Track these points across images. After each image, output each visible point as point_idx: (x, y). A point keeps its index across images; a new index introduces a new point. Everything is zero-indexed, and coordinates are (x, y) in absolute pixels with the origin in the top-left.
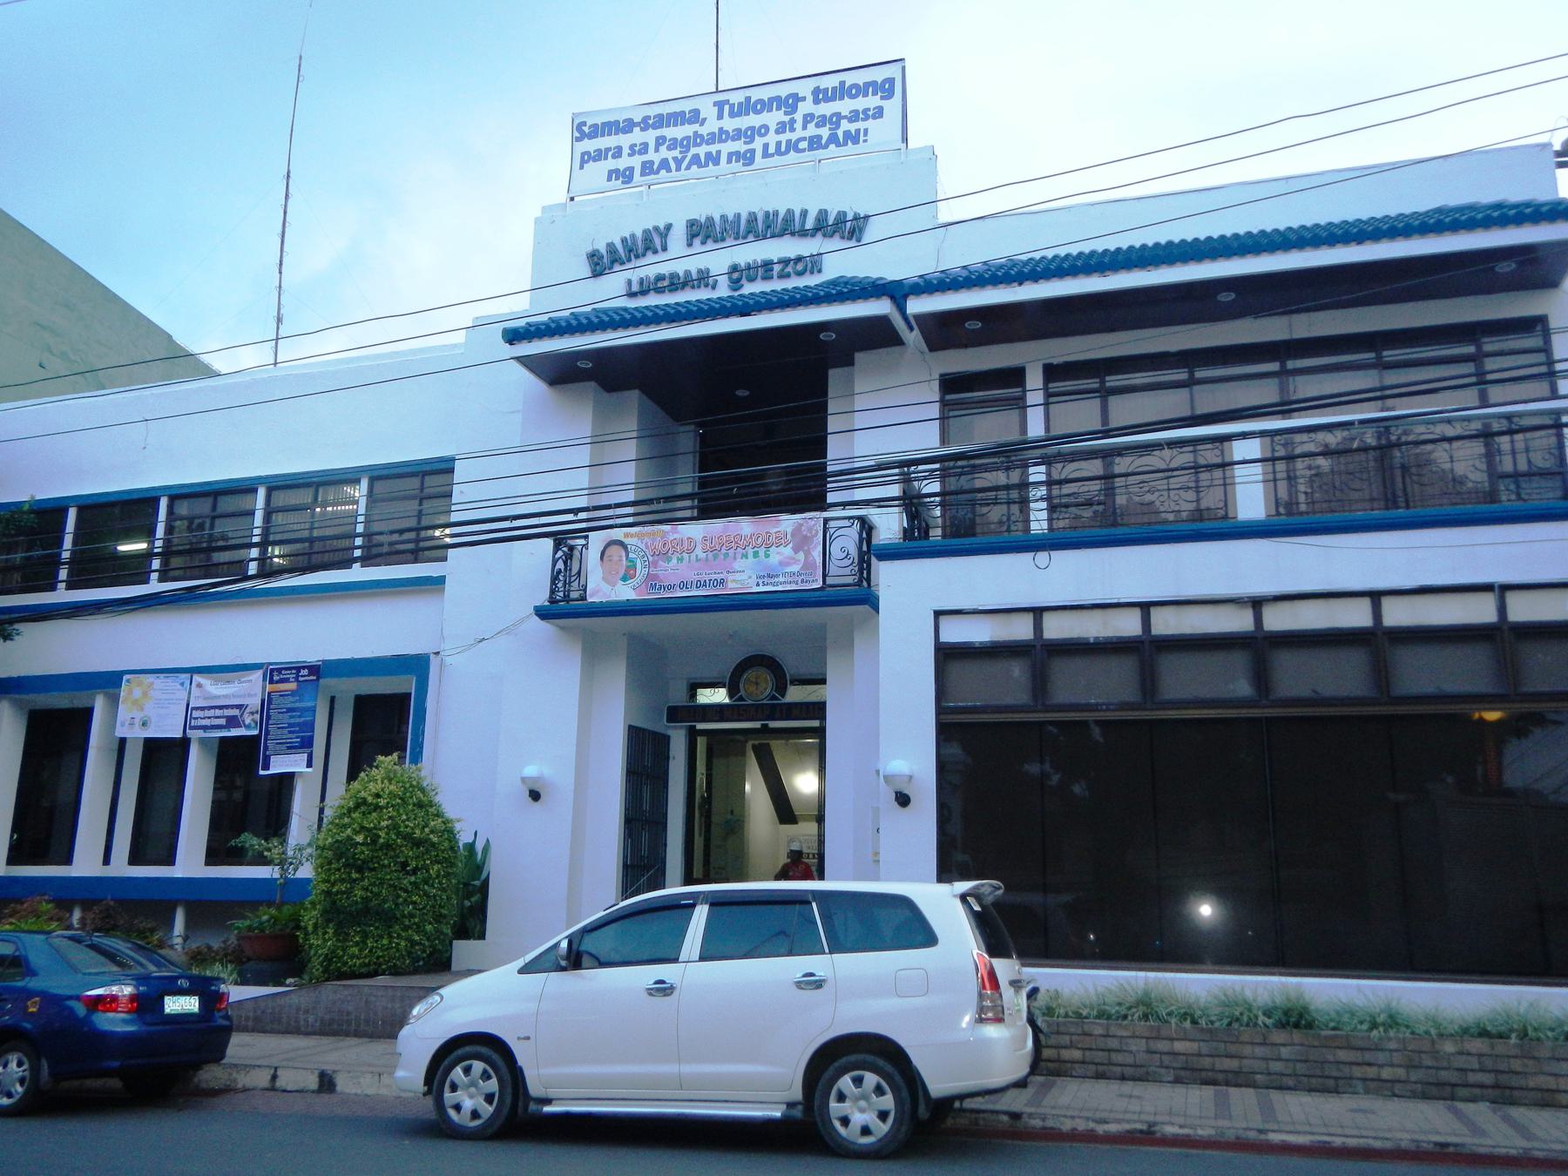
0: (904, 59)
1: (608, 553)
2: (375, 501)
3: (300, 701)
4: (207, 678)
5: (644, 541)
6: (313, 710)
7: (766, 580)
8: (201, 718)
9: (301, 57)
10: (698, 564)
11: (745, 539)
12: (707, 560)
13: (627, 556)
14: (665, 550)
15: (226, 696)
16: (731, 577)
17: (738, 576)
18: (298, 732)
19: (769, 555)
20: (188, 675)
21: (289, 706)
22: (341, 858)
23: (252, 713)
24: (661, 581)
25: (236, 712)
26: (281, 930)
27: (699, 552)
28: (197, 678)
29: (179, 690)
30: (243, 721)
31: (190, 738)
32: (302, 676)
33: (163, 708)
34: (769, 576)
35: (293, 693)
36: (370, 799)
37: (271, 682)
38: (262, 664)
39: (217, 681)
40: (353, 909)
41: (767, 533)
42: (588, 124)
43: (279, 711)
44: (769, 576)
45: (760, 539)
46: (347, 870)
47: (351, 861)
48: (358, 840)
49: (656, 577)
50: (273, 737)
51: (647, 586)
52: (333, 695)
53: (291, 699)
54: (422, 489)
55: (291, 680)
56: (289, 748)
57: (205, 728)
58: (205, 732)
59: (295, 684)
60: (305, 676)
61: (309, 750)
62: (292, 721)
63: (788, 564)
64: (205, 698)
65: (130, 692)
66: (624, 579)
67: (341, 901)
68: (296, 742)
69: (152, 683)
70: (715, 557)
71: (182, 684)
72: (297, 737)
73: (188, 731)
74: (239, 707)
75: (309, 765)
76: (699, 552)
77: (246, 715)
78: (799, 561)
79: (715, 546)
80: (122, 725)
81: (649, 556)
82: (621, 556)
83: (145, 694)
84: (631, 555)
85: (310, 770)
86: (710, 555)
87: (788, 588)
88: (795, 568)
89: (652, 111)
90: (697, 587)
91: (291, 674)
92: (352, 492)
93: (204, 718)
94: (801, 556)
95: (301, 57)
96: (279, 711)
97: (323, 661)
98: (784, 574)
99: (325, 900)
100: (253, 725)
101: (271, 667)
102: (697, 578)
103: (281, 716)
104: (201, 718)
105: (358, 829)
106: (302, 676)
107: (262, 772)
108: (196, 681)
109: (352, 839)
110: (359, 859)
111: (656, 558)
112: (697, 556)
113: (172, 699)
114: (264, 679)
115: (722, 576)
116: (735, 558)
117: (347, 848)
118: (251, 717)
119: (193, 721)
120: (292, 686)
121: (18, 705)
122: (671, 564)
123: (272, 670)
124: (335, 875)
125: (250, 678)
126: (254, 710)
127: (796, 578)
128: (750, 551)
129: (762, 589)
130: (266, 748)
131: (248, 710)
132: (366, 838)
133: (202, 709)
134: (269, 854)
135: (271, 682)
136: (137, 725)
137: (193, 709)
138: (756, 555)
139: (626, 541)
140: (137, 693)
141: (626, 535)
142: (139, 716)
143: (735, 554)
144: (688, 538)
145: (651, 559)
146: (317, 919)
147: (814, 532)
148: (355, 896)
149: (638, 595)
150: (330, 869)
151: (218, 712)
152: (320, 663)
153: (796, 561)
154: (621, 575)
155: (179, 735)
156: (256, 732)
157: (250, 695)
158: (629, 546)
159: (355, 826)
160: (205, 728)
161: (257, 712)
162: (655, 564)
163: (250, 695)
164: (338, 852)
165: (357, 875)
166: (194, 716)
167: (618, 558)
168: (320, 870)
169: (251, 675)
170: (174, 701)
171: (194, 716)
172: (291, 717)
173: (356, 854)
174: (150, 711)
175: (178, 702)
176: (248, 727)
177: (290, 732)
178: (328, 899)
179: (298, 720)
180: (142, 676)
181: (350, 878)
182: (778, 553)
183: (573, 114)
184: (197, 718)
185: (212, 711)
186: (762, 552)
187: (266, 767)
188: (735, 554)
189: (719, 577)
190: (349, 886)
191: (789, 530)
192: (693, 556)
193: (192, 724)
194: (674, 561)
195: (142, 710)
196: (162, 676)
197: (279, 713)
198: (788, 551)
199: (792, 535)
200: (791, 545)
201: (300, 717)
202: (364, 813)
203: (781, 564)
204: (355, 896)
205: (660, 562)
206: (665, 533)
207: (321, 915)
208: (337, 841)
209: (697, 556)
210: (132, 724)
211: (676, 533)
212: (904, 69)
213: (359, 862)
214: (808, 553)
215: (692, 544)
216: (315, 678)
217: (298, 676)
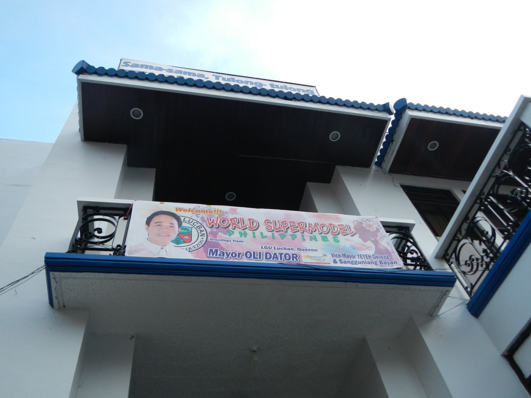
0: (315, 87)
1: (156, 219)
5: (200, 216)
7: (342, 258)
10: (264, 240)
11: (310, 226)
12: (273, 237)
13: (180, 225)
14: (226, 224)
16: (303, 254)
17: (311, 254)
19: (338, 241)
24: (222, 248)
27: (263, 228)
34: (344, 255)
41: (330, 225)
42: (131, 63)
44: (344, 255)
45: (325, 229)
49: (217, 245)
51: (206, 252)
63: (360, 249)
66: (177, 242)
70: (283, 237)
76: (263, 228)
78: (370, 247)
79: (279, 228)
81: (207, 228)
82: (172, 224)
84: (184, 224)
86: (276, 234)
87: (369, 266)
88: (371, 252)
89: (175, 69)
90: (266, 258)
94: (369, 243)
98: (360, 256)
102: (265, 251)
111: (215, 230)
112: (262, 233)
115: (293, 252)
116: (304, 240)
122: (232, 236)
127: (374, 260)
128: (319, 237)
129: (339, 265)
138: (325, 239)
139: (178, 213)
141: (180, 210)
143: (303, 236)
144: (250, 220)
145: (209, 230)
147: (375, 229)
149: (194, 256)
153: (368, 248)
154: (174, 236)
158: (182, 218)
162: (215, 235)
167: (168, 225)
182: (347, 240)
183: (123, 58)
186: (330, 236)
188: (303, 236)
189: (291, 252)
191: (352, 226)
192: (257, 233)
194: (236, 235)
198: (357, 239)
199: (355, 228)
200: (357, 235)
203: (354, 248)
205: (220, 233)
206: (222, 213)
209: (262, 233)
211: (236, 214)
212: (316, 89)
214: (376, 243)
215: (255, 224)
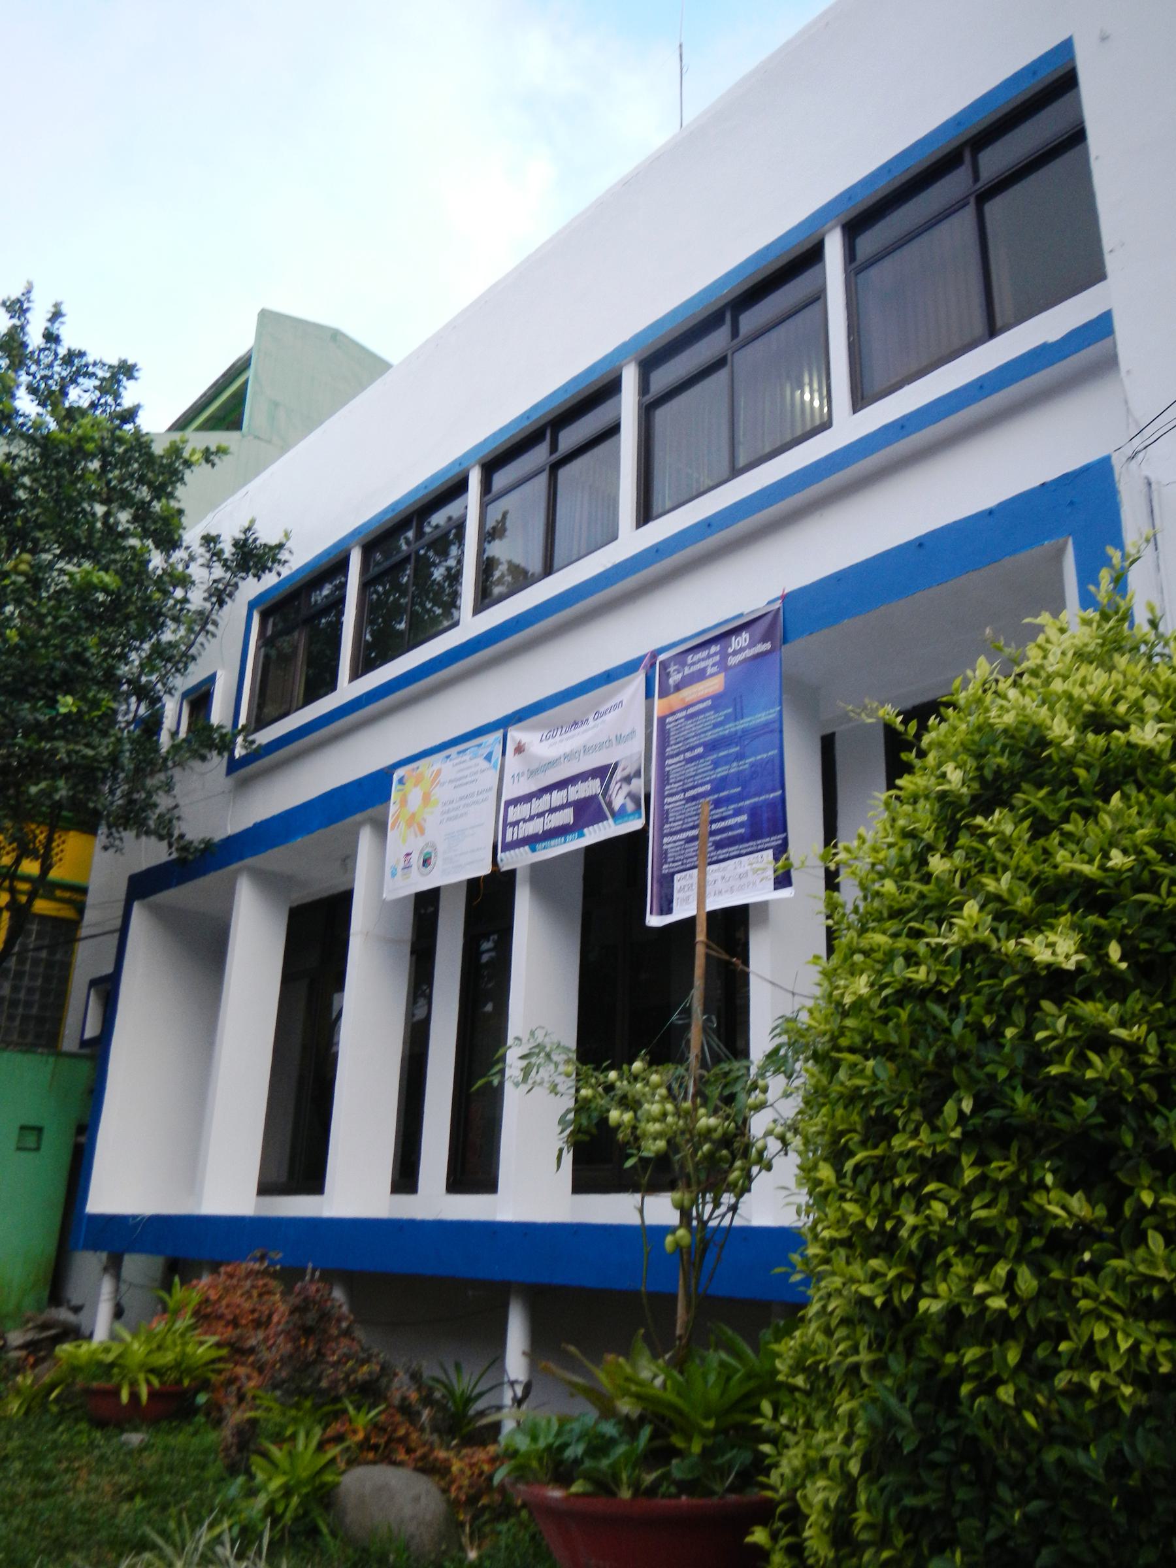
2: (859, 271)
3: (737, 716)
4: (533, 728)
6: (775, 730)
8: (525, 821)
9: (681, 46)
15: (568, 757)
18: (740, 797)
20: (499, 734)
21: (709, 736)
22: (948, 1090)
23: (627, 780)
25: (592, 787)
26: (685, 1487)
28: (516, 734)
29: (483, 771)
30: (609, 804)
31: (512, 873)
32: (735, 653)
33: (456, 817)
35: (717, 701)
36: (1061, 730)
37: (662, 695)
38: (640, 660)
39: (556, 728)
40: (1091, 1458)
43: (688, 755)
46: (1001, 1168)
47: (1021, 1100)
48: (1043, 956)
50: (677, 826)
52: (828, 731)
53: (713, 717)
54: (976, 179)
55: (709, 671)
56: (718, 845)
57: (532, 841)
58: (533, 850)
59: (722, 676)
60: (742, 650)
61: (776, 840)
62: (722, 772)
64: (532, 773)
65: (404, 802)
67: (989, 1387)
68: (741, 825)
69: (439, 772)
71: (488, 758)
72: (737, 813)
73: (500, 855)
74: (602, 773)
75: (783, 880)
77: (614, 787)
80: (393, 875)
83: (426, 798)
85: (786, 893)
91: (709, 656)
92: (816, 403)
93: (531, 818)
95: (681, 46)
96: (688, 755)
97: (784, 598)
99: (879, 1368)
100: (630, 806)
101: (662, 657)
103: (691, 769)
104: (525, 821)
105: (1024, 901)
106: (735, 653)
107: (654, 921)
108: (512, 737)
109: (997, 965)
110: (1070, 1086)
113: (472, 795)
114: (649, 694)
117: (976, 1027)
118: (626, 789)
119: (509, 830)
120: (714, 685)
121: (269, 882)
123: (664, 665)
124: (921, 1203)
125: (616, 700)
126: (630, 770)
130: (663, 856)
131: (619, 775)
132: (1093, 944)
133: (527, 798)
134: (628, 1116)
135: (662, 695)
136: (414, 869)
137: (509, 803)
140: (415, 795)
142: (417, 846)
146: (850, 1486)
148: (1089, 1357)
150: (882, 1170)
151: (558, 797)
152: (778, 604)
155: (485, 869)
156: (636, 824)
157: (620, 739)
159: (1003, 883)
160: (532, 841)
161: (637, 774)
163: (620, 739)
164: (924, 1055)
165: (1077, 1202)
166: (511, 819)
168: (826, 1172)
169: (623, 687)
170: (475, 799)
171: (511, 819)
172: (716, 764)
173: (1038, 1058)
174: (436, 832)
175: (481, 797)
176: (619, 815)
177: (717, 804)
178: (896, 1364)
179: (734, 768)
180: (422, 763)
181: (1034, 1222)
184: (517, 823)
185: (546, 797)
187: (666, 907)
190: (1027, 1282)
193: (509, 839)
195: (422, 831)
196: (453, 751)
197: (689, 761)
201: (740, 757)
202: (1041, 827)
204: (1089, 1357)
207: (865, 1467)
208: (907, 992)
210: (407, 867)
213: (1084, 1105)
216: (767, 646)
217: (725, 656)
